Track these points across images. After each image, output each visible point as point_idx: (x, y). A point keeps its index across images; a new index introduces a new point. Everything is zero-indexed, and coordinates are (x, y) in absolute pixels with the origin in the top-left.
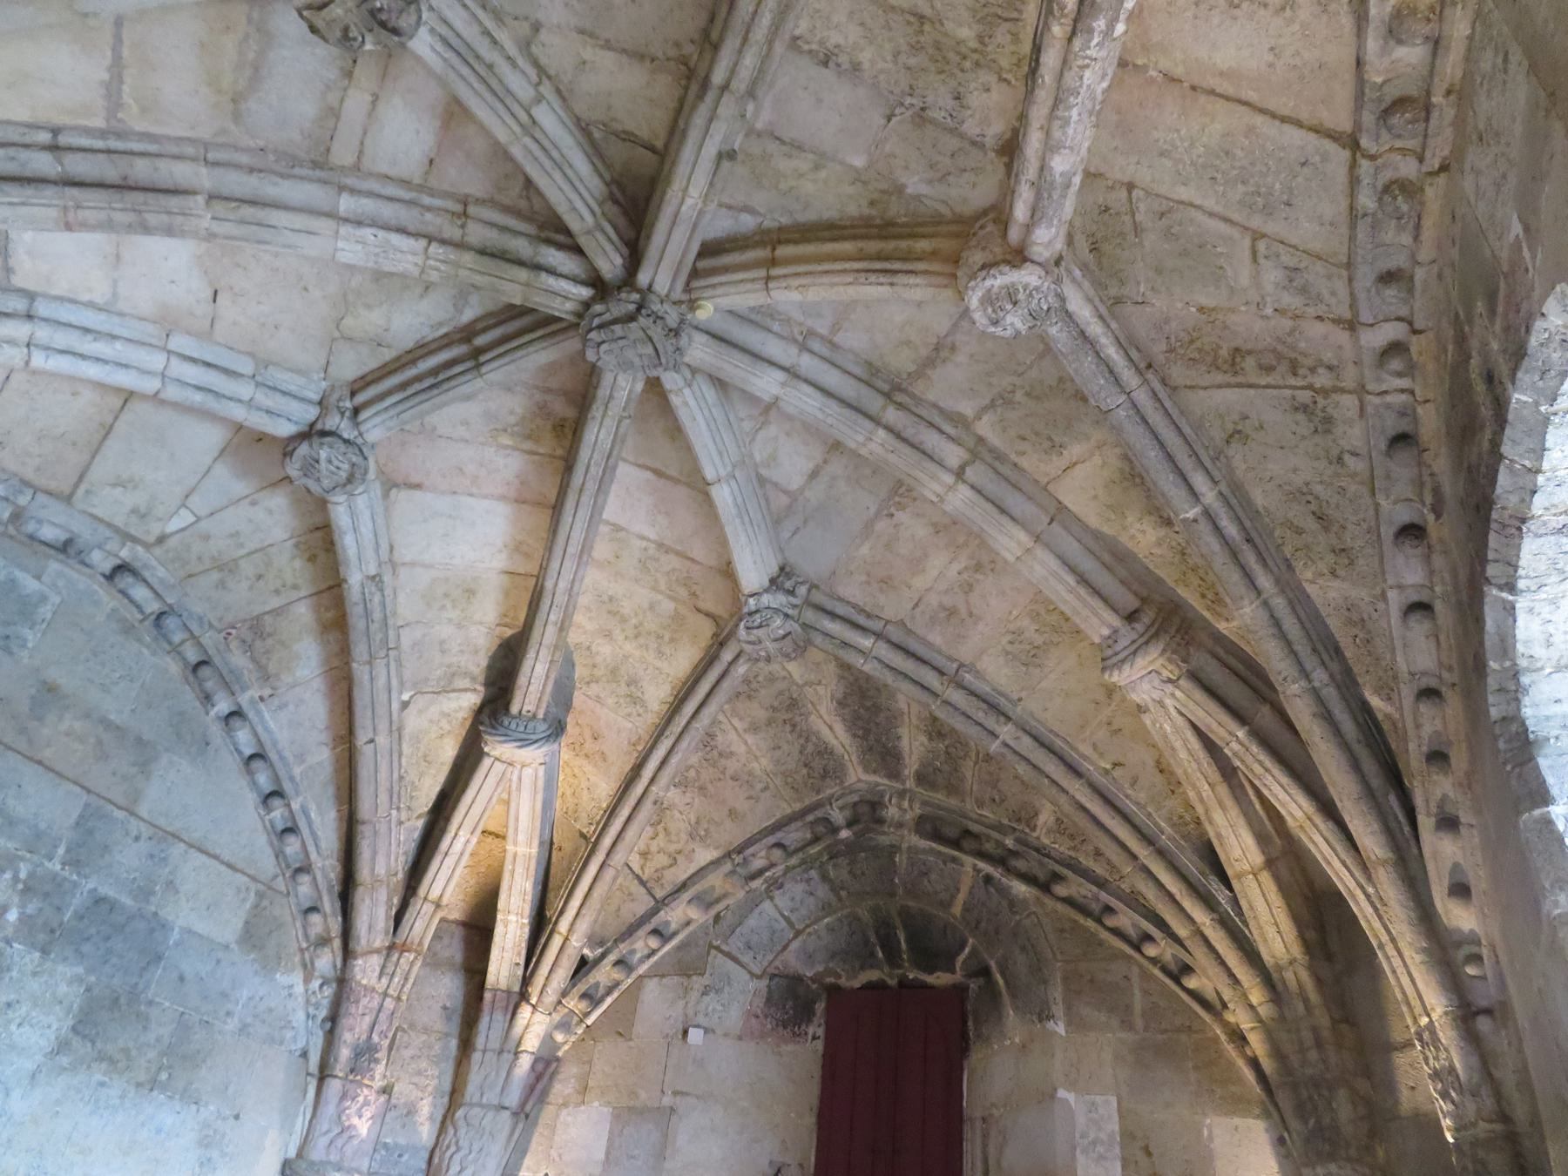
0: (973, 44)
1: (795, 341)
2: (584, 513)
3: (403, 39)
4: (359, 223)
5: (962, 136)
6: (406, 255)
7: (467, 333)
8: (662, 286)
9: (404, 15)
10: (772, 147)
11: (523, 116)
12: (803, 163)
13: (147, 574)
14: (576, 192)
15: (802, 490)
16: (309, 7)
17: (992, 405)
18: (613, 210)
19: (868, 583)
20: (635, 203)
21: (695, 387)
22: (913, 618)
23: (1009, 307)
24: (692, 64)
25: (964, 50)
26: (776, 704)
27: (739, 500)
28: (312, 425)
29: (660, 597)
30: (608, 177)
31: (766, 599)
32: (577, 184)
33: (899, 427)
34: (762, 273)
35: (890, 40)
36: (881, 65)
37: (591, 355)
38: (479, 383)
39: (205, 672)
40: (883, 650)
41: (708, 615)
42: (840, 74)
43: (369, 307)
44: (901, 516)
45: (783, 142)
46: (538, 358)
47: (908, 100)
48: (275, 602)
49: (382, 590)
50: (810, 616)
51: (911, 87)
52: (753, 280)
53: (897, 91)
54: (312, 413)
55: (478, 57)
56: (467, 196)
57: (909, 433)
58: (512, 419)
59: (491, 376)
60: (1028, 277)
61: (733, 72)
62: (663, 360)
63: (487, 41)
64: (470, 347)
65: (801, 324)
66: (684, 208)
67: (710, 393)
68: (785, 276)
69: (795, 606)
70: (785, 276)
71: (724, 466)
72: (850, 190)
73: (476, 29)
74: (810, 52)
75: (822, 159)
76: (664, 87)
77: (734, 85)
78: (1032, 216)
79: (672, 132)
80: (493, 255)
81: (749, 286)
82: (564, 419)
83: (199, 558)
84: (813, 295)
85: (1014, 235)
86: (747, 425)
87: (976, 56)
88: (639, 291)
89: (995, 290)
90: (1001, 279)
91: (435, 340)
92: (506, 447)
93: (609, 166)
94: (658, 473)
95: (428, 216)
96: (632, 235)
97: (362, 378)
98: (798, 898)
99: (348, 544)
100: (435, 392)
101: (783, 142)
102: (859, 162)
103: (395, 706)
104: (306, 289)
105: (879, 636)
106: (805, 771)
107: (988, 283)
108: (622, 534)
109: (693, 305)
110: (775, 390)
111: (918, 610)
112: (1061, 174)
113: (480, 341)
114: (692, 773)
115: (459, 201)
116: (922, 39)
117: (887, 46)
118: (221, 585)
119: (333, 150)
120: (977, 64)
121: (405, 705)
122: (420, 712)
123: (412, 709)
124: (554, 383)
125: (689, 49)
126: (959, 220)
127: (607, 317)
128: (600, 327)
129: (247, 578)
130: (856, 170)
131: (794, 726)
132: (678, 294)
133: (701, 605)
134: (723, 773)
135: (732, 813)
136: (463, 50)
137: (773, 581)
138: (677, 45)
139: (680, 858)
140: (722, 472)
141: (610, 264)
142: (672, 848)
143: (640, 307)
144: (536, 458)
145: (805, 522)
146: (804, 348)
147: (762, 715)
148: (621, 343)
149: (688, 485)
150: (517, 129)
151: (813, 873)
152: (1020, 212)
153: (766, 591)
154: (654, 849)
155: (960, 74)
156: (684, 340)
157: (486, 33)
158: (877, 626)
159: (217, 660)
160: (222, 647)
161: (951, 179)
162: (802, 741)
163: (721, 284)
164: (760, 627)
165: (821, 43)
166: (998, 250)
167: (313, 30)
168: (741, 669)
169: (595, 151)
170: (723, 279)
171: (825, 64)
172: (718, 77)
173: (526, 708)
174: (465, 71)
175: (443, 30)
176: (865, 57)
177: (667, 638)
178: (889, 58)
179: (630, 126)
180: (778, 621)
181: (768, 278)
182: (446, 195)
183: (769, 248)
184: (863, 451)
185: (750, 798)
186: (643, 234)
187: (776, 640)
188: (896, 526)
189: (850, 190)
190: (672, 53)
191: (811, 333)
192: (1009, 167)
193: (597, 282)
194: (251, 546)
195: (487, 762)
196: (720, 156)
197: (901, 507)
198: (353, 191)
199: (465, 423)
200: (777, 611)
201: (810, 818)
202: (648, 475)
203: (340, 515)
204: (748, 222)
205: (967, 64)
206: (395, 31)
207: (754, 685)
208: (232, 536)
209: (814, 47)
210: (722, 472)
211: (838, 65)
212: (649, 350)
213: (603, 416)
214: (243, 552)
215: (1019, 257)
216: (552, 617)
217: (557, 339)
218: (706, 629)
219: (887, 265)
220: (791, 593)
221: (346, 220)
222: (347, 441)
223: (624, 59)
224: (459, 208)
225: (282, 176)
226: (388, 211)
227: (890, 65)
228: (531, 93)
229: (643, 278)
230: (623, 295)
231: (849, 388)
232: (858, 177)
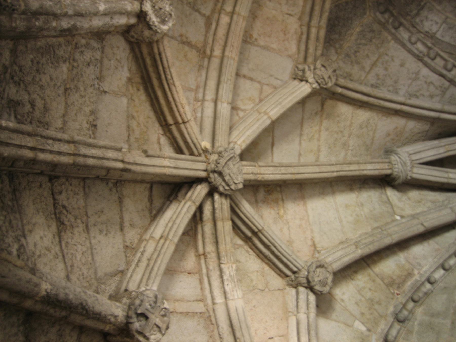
0: (67, 64)
1: (202, 105)
2: (302, 170)
3: (157, 293)
4: (225, 293)
5: (102, 58)
6: (229, 270)
7: (247, 240)
8: (202, 166)
9: (149, 295)
10: (132, 139)
11: (162, 241)
12: (134, 124)
13: (385, 331)
14: (178, 214)
15: (259, 82)
16: (160, 331)
17: (198, 11)
18: (180, 195)
19: (287, 39)
20: (175, 188)
21: (235, 140)
22: (296, 14)
23: (163, 10)
24: (115, 181)
25: (71, 68)
26: (350, 63)
27: (273, 106)
28: (306, 287)
29: (322, 128)
30: (168, 202)
31: (311, 80)
32: (177, 212)
33: (221, 47)
34: (182, 126)
35: (77, 101)
36: (88, 102)
37: (241, 186)
38: (266, 228)
39: (416, 298)
40: (314, 22)
41: (323, 105)
42: (97, 118)
43: (252, 281)
44: (255, 36)
45: (129, 135)
46: (247, 208)
47: (97, 86)
48: (378, 281)
49: (360, 241)
50: (310, 59)
51: (91, 86)
52: (186, 129)
53: (95, 92)
54: (301, 289)
55: (148, 265)
56: (196, 256)
57: (222, 42)
58: (272, 211)
59: (262, 224)
60: (148, 7)
61: (116, 160)
62: (232, 155)
63: (140, 264)
64: (250, 236)
65: (194, 105)
66: (172, 165)
67: (235, 133)
68: (180, 115)
69: (309, 67)
70: (180, 115)
71: (262, 117)
72: (137, 101)
73: (138, 269)
74: (93, 134)
75: (130, 117)
76: (127, 191)
77: (120, 158)
78: (124, 14)
79: (142, 182)
80: (216, 238)
81: (190, 130)
82: (265, 191)
83: (371, 314)
84: (184, 101)
85: (133, 21)
86: (241, 114)
87: (71, 61)
88: (209, 174)
89: (158, 20)
90: (153, 19)
91: (254, 252)
92: (285, 211)
93: (164, 204)
94: (273, 145)
95: (211, 268)
96: (186, 185)
97: (279, 275)
98: (430, 23)
99: (347, 260)
100: (276, 245)
101: (129, 135)
102: (125, 100)
103: (404, 220)
104: (254, 306)
105: (309, 27)
106: (374, 40)
107: (156, 24)
108: (302, 152)
109: (206, 151)
110: (225, 105)
111: (292, 13)
112: (105, 5)
113: (249, 234)
114: (391, 88)
115: (200, 259)
116: (73, 87)
117: (80, 101)
118: (379, 303)
119: (200, 311)
120: (74, 60)
121: (402, 217)
122: (402, 210)
123: (403, 213)
124: (253, 200)
125: (111, 185)
126: (132, 50)
127: (223, 184)
128: (228, 185)
129: (372, 294)
130: (129, 100)
131: (356, 52)
132: (203, 158)
133: (320, 109)
134: (386, 75)
135: (402, 65)
136: (148, 271)
137: (302, 80)
138: (111, 190)
139: (429, 80)
140: (265, 117)
141: (201, 191)
142: (425, 86)
143: (214, 171)
144: (284, 197)
145: (271, 76)
146: (203, 100)
147: (356, 68)
148: (232, 175)
149: (273, 132)
150: (168, 242)
151: (418, 20)
152: (123, 21)
153: (307, 81)
154: (428, 94)
155: (80, 66)
156: (221, 149)
157: (137, 265)
158: (305, 29)
159: (409, 295)
160: (404, 295)
161: (118, 58)
162: (361, 46)
163: (192, 141)
164: (323, 79)
165: (88, 130)
166: (141, 26)
167: (167, 328)
168: (342, 81)
169: (160, 211)
170: (189, 141)
171: (95, 126)
172: (120, 165)
173: (387, 167)
174: (156, 268)
175: (145, 280)
176: (87, 110)
177: (338, 119)
178: (84, 99)
179: (146, 200)
180: (318, 72)
181: (184, 123)
182: (199, 264)
183: (171, 127)
184: (236, 58)
185: (393, 60)
186: (185, 181)
187: (326, 70)
188: (260, 36)
190: (114, 190)
191: (196, 100)
192: (108, 33)
193: (210, 194)
194: (359, 297)
195: (415, 176)
196: (148, 156)
198: (213, 299)
199: (281, 230)
200: (314, 74)
201: (393, 31)
202: (275, 149)
203: (337, 266)
204: (164, 140)
205: (75, 64)
206: (156, 297)
207: (345, 75)
208: (358, 305)
209: (91, 132)
210: (265, 117)
211: (94, 120)
212: (230, 163)
214: (363, 299)
215: (141, 16)
216: (347, 169)
217: (237, 202)
218: (329, 103)
219: (162, 73)
220: (303, 71)
221: (226, 298)
222: (308, 272)
223: (124, 209)
224: (202, 257)
225: (218, 326)
226: (216, 283)
227: (87, 98)
228: (151, 241)
229: (203, 174)
230: (213, 180)
231: (213, 74)
232: (131, 99)
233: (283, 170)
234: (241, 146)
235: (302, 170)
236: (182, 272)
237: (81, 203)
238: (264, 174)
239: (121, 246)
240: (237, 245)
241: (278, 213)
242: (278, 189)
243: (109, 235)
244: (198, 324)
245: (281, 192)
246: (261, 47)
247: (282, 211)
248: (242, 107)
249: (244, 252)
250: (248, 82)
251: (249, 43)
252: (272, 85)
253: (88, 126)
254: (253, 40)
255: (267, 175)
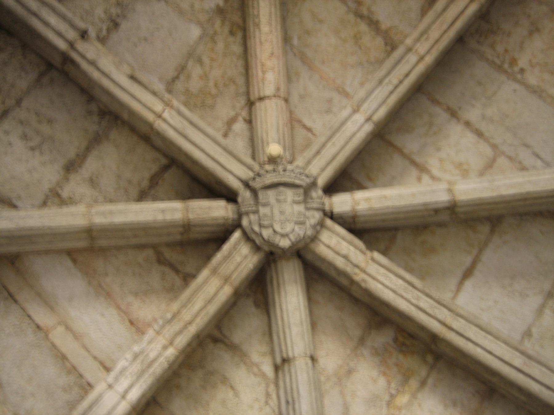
12: (196, 71)
15: (494, 147)
42: (125, 17)
44: (523, 62)
58: (382, 382)
72: (220, 46)
92: (410, 404)
94: (468, 274)
102: (196, 32)
108: (534, 330)
128: (261, 226)
144: (430, 381)
145: (526, 146)
148: (276, 212)
149: (480, 251)
172: (62, 45)
179: (147, 175)
188: (532, 66)
189: (220, 46)
197: (513, 62)
202: (468, 284)
209: (105, 27)
213: (364, 272)
223: (95, 153)
229: (235, 184)
233: (425, 303)
234: (358, 204)
235: (472, 332)
236: (118, 307)
237: (23, 83)
238: (374, 278)
239: (46, 186)
240: (260, 370)
241: (392, 396)
242: (430, 358)
243: (37, 153)
244: (65, 390)
245: (432, 367)
246: (527, 86)
247: (403, 399)
248: (435, 172)
249: (261, 389)
250: (470, 138)
251: (505, 72)
252: (520, 163)
253: (103, 15)
254: (516, 69)
255: (380, 286)
